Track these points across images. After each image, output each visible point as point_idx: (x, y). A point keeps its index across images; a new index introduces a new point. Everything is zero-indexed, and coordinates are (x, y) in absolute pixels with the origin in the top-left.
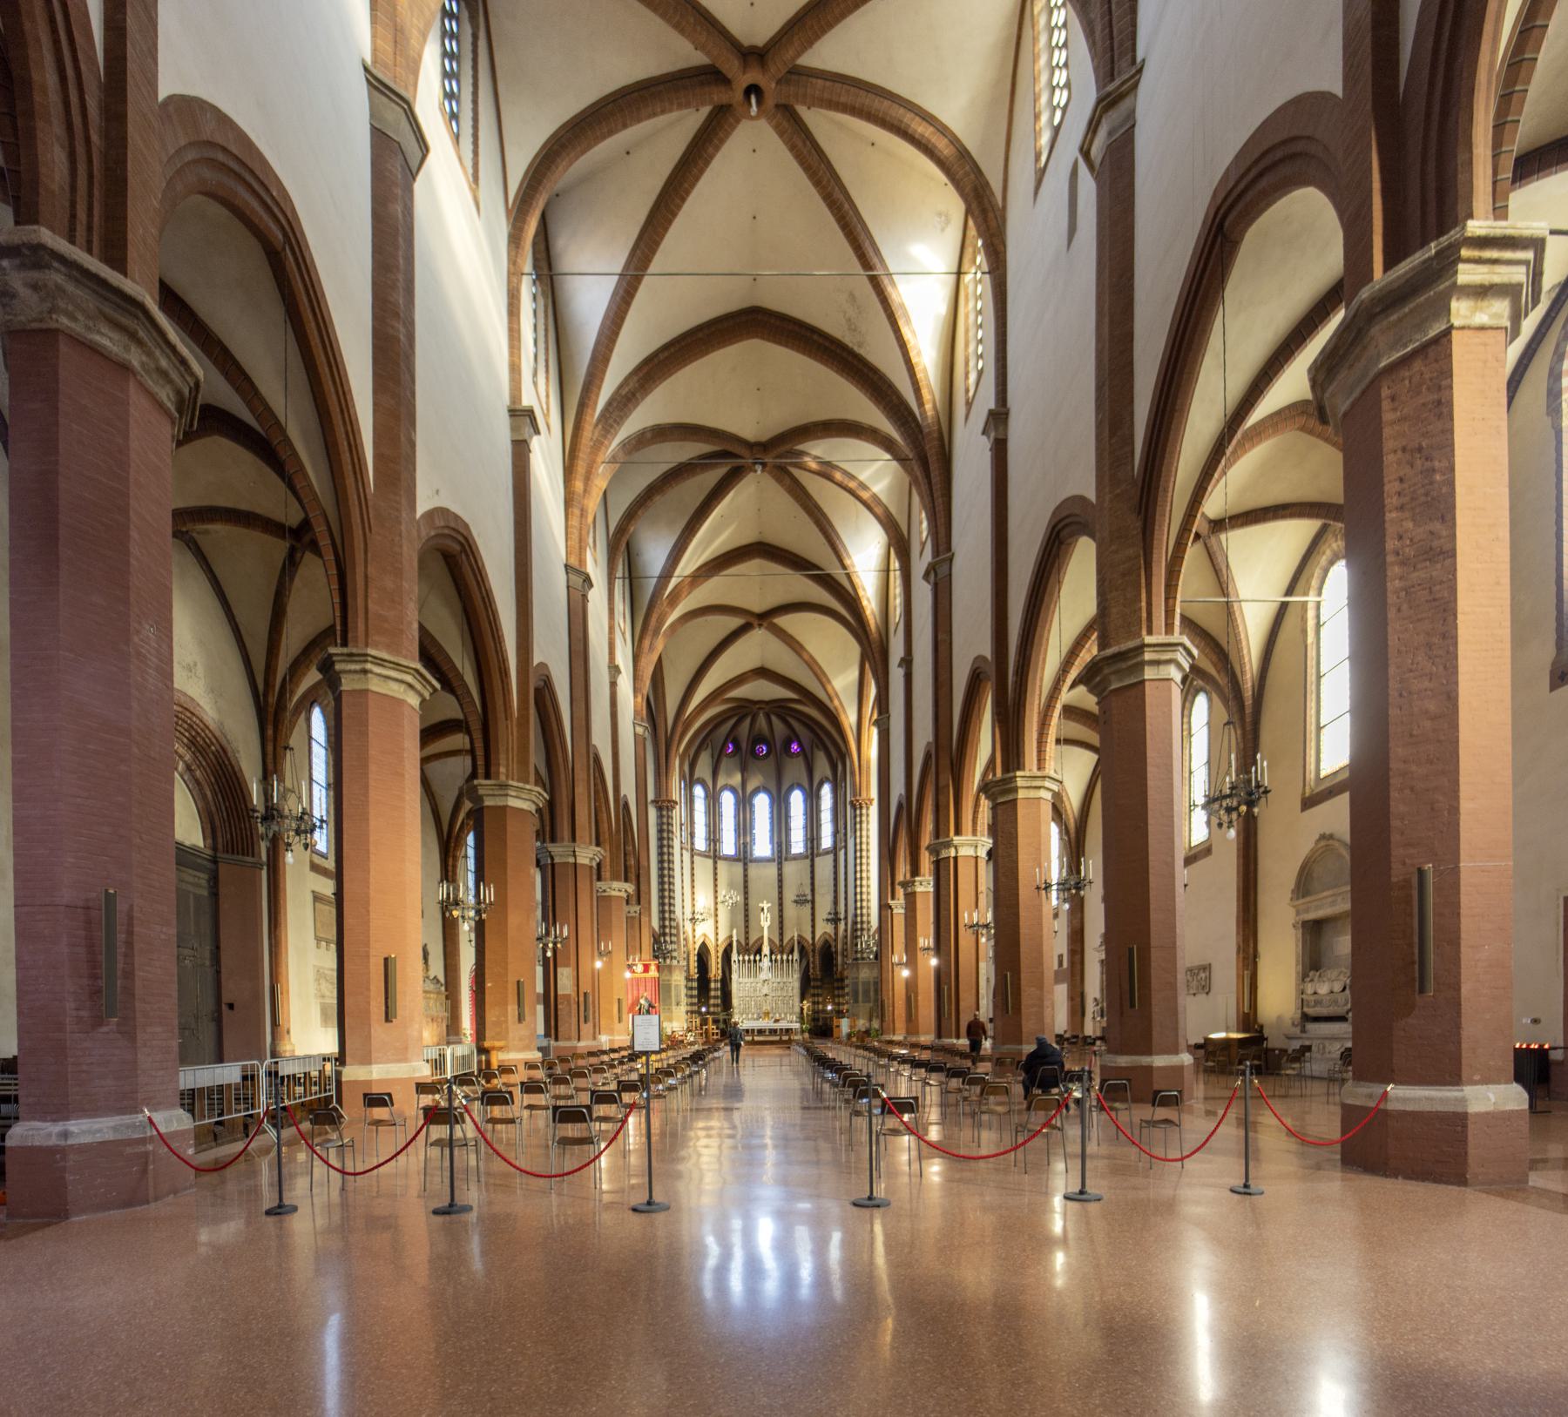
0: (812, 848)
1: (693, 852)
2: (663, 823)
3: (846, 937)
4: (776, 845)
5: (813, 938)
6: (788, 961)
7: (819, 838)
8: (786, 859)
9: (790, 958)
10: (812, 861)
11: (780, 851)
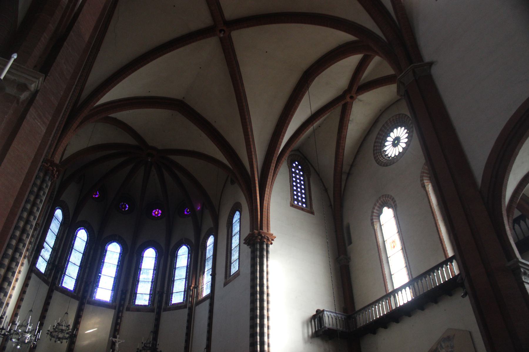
0: (160, 301)
1: (32, 269)
4: (119, 293)
7: (170, 293)
8: (128, 309)
10: (159, 315)
11: (123, 299)
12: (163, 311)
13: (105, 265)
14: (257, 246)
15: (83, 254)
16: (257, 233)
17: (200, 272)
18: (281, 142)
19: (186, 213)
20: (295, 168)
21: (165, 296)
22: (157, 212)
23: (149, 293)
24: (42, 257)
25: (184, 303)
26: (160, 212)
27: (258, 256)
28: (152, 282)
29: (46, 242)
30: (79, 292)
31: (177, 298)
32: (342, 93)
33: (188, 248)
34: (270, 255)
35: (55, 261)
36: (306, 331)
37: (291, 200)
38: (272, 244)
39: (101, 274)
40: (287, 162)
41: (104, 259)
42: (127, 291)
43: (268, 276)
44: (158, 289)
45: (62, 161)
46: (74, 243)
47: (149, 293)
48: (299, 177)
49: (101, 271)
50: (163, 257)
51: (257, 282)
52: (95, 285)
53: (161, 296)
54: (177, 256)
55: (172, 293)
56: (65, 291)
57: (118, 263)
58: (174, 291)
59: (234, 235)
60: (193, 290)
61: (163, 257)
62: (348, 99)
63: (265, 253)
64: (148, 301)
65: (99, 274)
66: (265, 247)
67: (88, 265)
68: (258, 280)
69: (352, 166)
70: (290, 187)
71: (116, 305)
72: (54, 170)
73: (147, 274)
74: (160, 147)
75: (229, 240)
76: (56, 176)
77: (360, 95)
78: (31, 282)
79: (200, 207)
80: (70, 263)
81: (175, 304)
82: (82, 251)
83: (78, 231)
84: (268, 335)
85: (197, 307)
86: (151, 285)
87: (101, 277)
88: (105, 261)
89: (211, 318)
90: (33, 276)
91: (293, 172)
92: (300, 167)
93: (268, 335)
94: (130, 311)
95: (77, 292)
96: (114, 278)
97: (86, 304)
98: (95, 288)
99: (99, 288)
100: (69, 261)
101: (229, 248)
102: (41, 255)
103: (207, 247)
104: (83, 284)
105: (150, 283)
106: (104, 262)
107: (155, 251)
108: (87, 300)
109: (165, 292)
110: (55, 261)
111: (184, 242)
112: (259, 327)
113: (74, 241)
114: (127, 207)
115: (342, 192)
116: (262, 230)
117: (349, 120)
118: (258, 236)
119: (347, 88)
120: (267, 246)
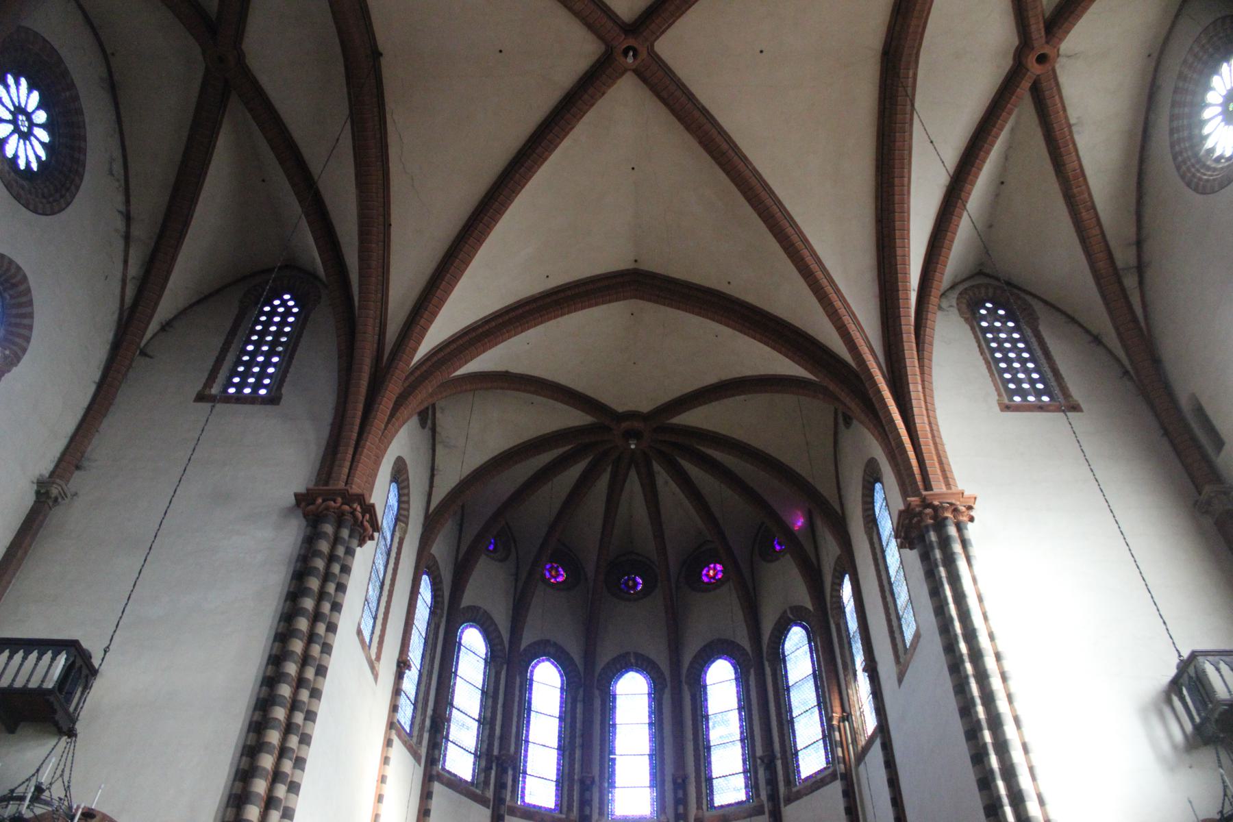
0: (772, 782)
2: (318, 553)
4: (669, 786)
7: (790, 755)
12: (785, 806)
13: (620, 731)
14: (930, 537)
16: (918, 503)
17: (845, 676)
18: (906, 256)
19: (778, 548)
20: (989, 319)
21: (779, 763)
22: (713, 571)
23: (741, 771)
24: (454, 743)
25: (829, 767)
26: (719, 567)
28: (742, 740)
29: (456, 708)
30: (570, 808)
31: (811, 761)
32: (1011, 62)
34: (974, 551)
35: (490, 745)
36: (1159, 731)
37: (999, 395)
38: (972, 519)
39: (615, 755)
40: (959, 310)
41: (614, 718)
42: (685, 779)
43: (983, 604)
44: (759, 752)
45: (430, 511)
46: (530, 698)
47: (741, 769)
48: (1007, 332)
49: (614, 748)
50: (752, 671)
51: (954, 631)
52: (606, 785)
54: (784, 656)
57: (650, 717)
59: (887, 545)
61: (752, 671)
62: (1035, 69)
63: (957, 548)
64: (744, 791)
65: (611, 756)
66: (952, 531)
67: (578, 741)
69: (1139, 243)
70: (985, 366)
71: (668, 819)
72: (355, 510)
74: (645, 407)
75: (880, 561)
76: (366, 523)
77: (1061, 40)
78: (435, 804)
80: (531, 745)
81: (811, 777)
83: (534, 667)
85: (862, 766)
86: (743, 748)
87: (617, 762)
88: (618, 721)
89: (893, 782)
90: (437, 787)
91: (985, 331)
92: (1001, 312)
95: (565, 809)
98: (609, 792)
99: (616, 789)
100: (527, 742)
103: (844, 608)
104: (575, 787)
105: (739, 745)
106: (614, 725)
107: (731, 663)
109: (779, 755)
110: (490, 745)
111: (791, 616)
112: (996, 754)
113: (530, 693)
114: (639, 584)
115: (1143, 324)
116: (932, 490)
117: (1070, 126)
119: (1017, 43)
120: (960, 527)
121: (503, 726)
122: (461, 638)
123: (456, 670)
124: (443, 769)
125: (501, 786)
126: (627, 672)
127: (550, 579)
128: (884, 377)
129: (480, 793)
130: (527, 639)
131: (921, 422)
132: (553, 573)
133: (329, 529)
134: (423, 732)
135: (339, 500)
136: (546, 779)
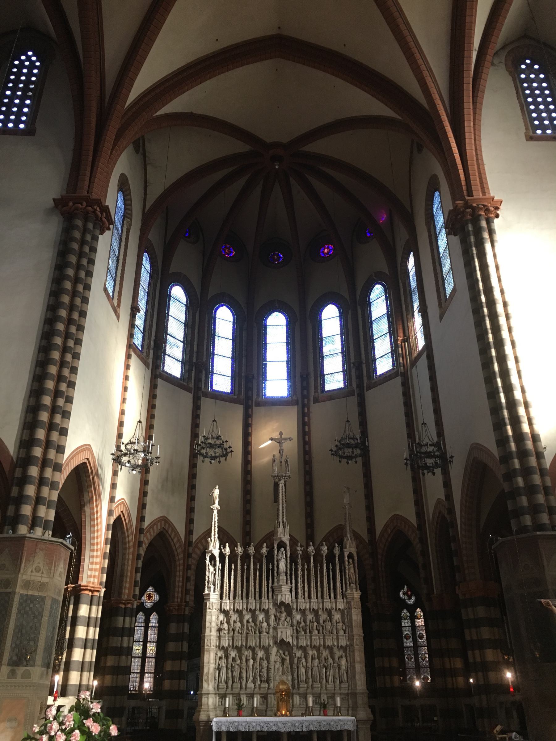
0: (360, 377)
3: (451, 510)
4: (298, 379)
5: (371, 530)
6: (331, 557)
7: (372, 361)
8: (316, 401)
9: (337, 551)
14: (468, 227)
15: (233, 340)
16: (462, 205)
21: (364, 366)
24: (169, 356)
25: (394, 369)
27: (473, 243)
29: (169, 335)
30: (240, 391)
33: (383, 285)
34: (498, 237)
38: (497, 216)
40: (506, 65)
42: (308, 375)
44: (352, 360)
47: (341, 370)
49: (266, 357)
50: (350, 311)
52: (261, 379)
53: (359, 368)
55: (375, 360)
56: (219, 396)
57: (287, 339)
58: (377, 356)
59: (439, 233)
60: (401, 345)
61: (350, 311)
63: (486, 235)
66: (484, 224)
68: (481, 284)
71: (297, 398)
72: (96, 210)
73: (333, 342)
74: (285, 140)
75: (434, 244)
76: (104, 219)
79: (385, 216)
80: (216, 356)
81: (383, 374)
82: (231, 337)
84: (519, 372)
86: (342, 357)
87: (268, 366)
89: (433, 378)
90: (160, 381)
93: (519, 372)
94: (319, 402)
95: (237, 393)
96: (286, 361)
97: (254, 407)
100: (213, 354)
101: (436, 257)
102: (167, 353)
105: (340, 355)
106: (266, 344)
108: (254, 400)
109: (364, 362)
110: (191, 357)
112: (498, 363)
116: (473, 196)
118: (466, 209)
120: (489, 222)
121: (198, 345)
122: (170, 292)
123: (168, 311)
124: (163, 371)
125: (198, 380)
126: (274, 312)
127: (225, 255)
128: (447, 117)
129: (186, 384)
130: (212, 291)
131: (470, 149)
132: (227, 251)
133: (79, 223)
134: (150, 349)
135: (84, 203)
136: (225, 376)
